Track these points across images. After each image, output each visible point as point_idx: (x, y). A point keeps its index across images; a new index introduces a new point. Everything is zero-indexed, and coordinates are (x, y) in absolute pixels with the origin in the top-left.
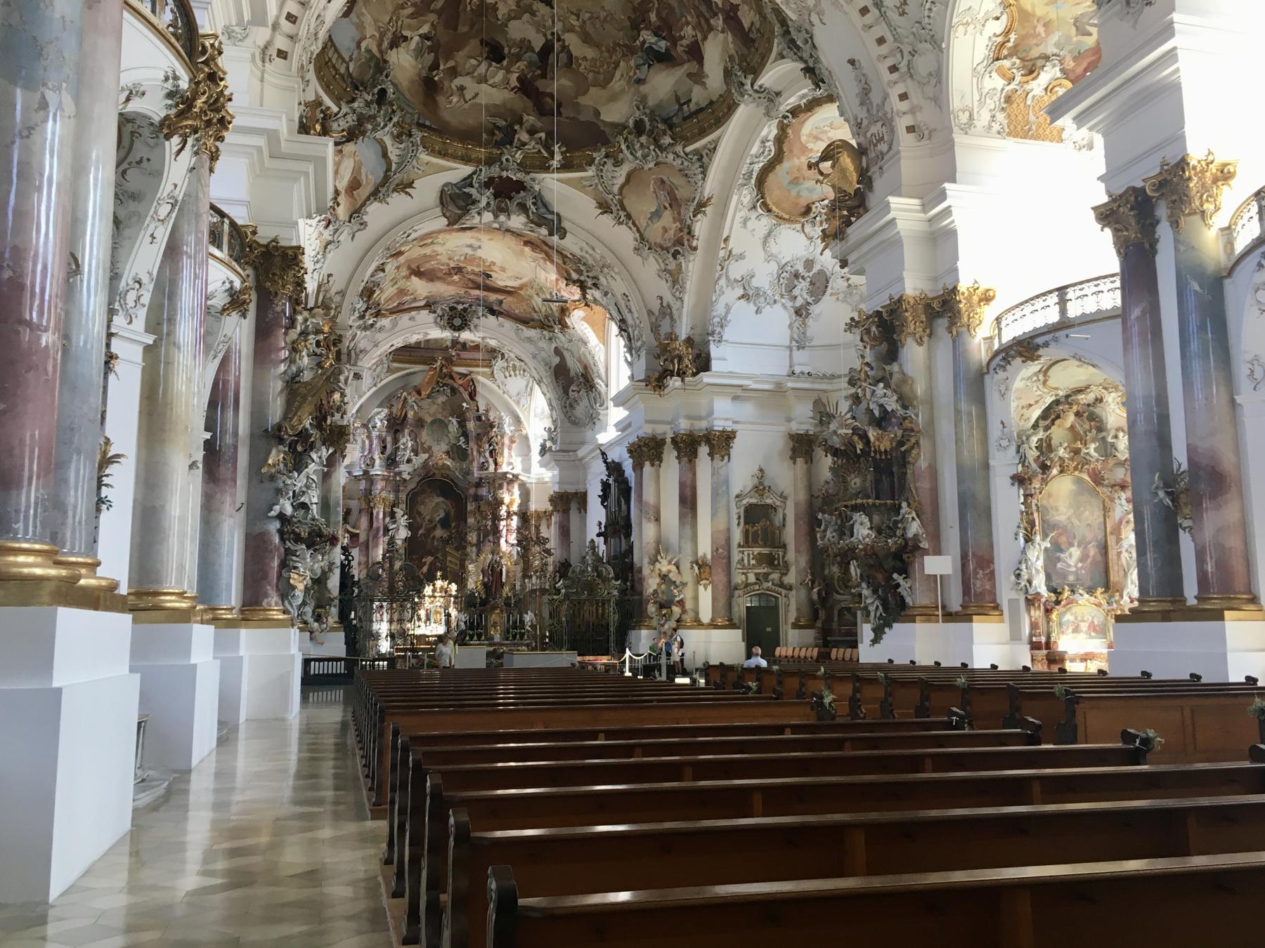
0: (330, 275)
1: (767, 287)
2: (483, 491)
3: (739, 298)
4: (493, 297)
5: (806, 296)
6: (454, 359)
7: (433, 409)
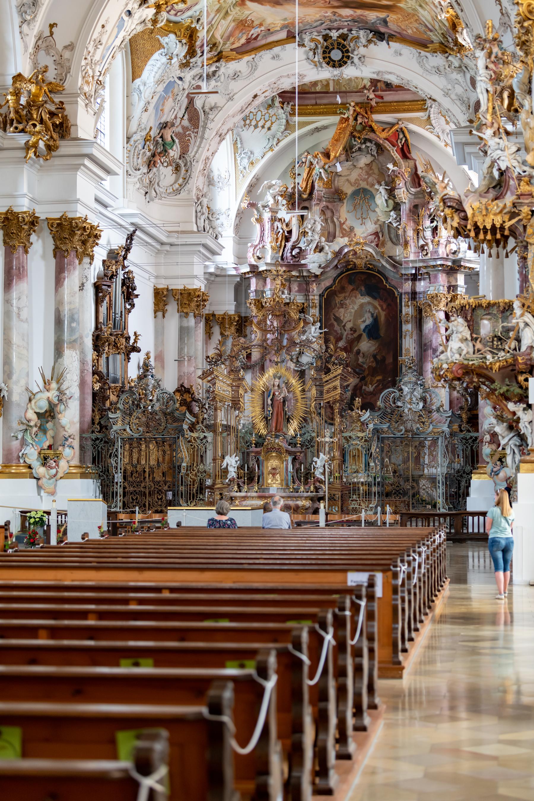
0: (52, 26)
2: (421, 286)
4: (372, 16)
6: (373, 103)
7: (354, 175)
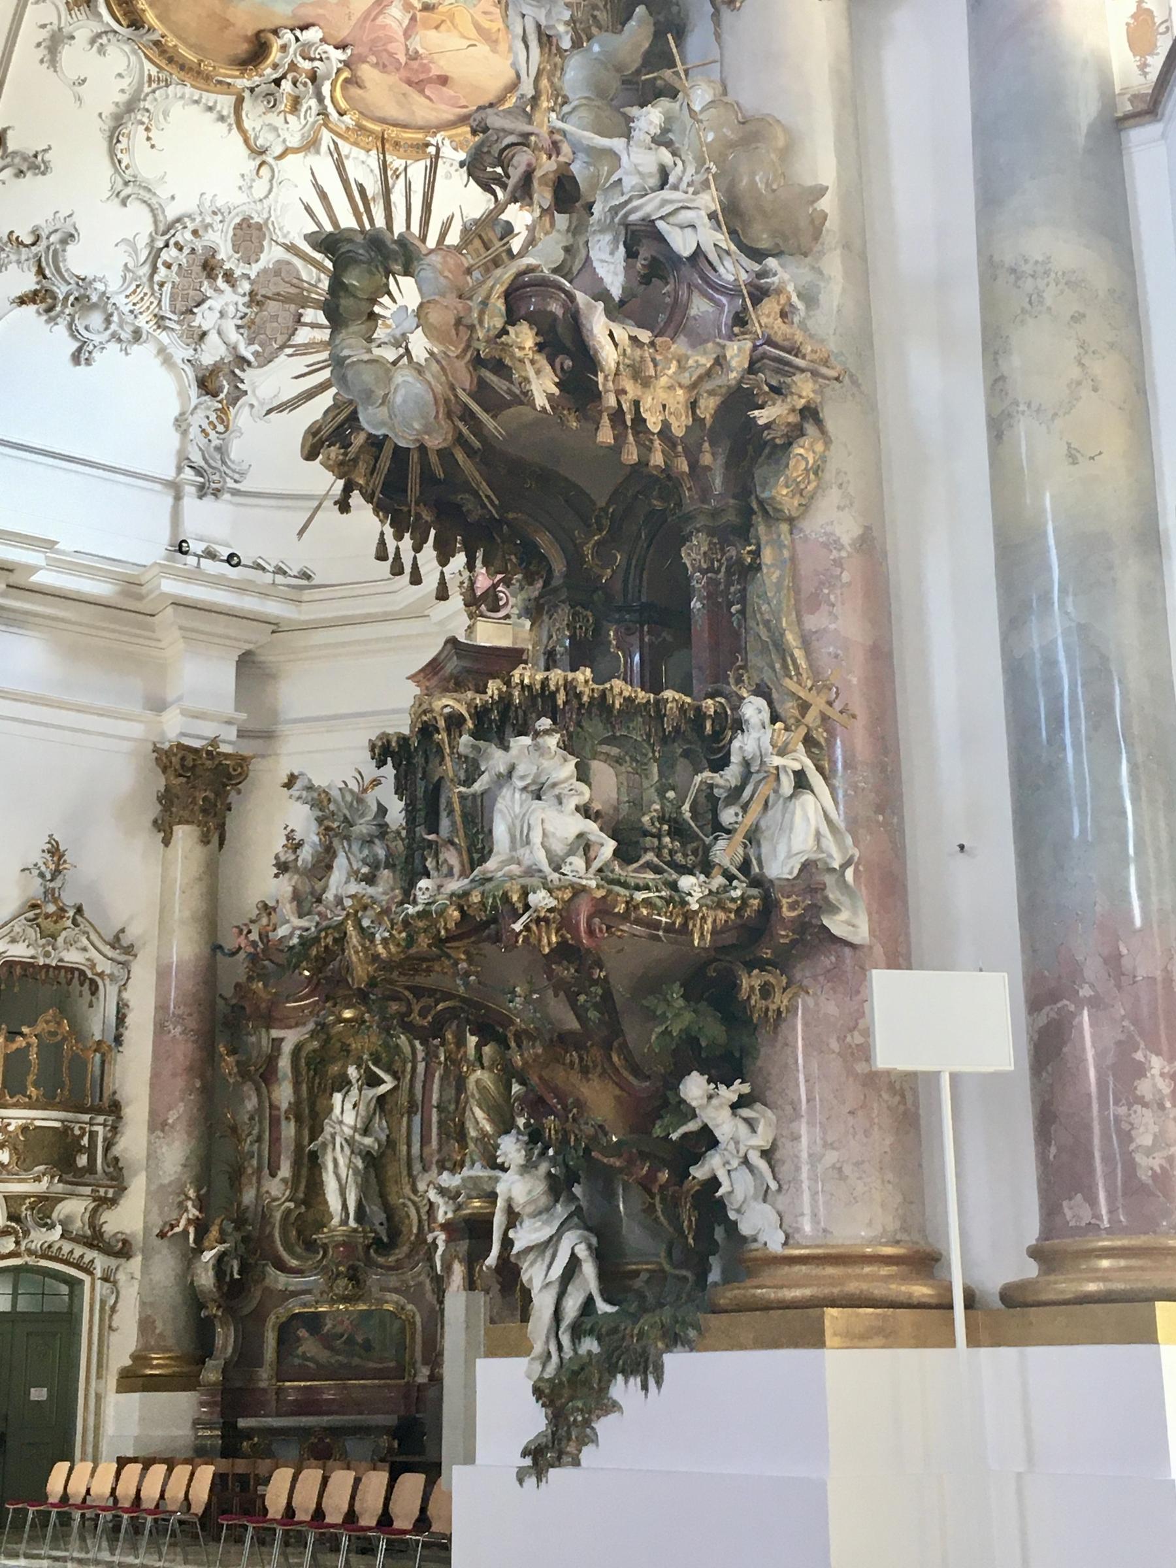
1: (113, 284)
3: (22, 301)
5: (233, 336)
